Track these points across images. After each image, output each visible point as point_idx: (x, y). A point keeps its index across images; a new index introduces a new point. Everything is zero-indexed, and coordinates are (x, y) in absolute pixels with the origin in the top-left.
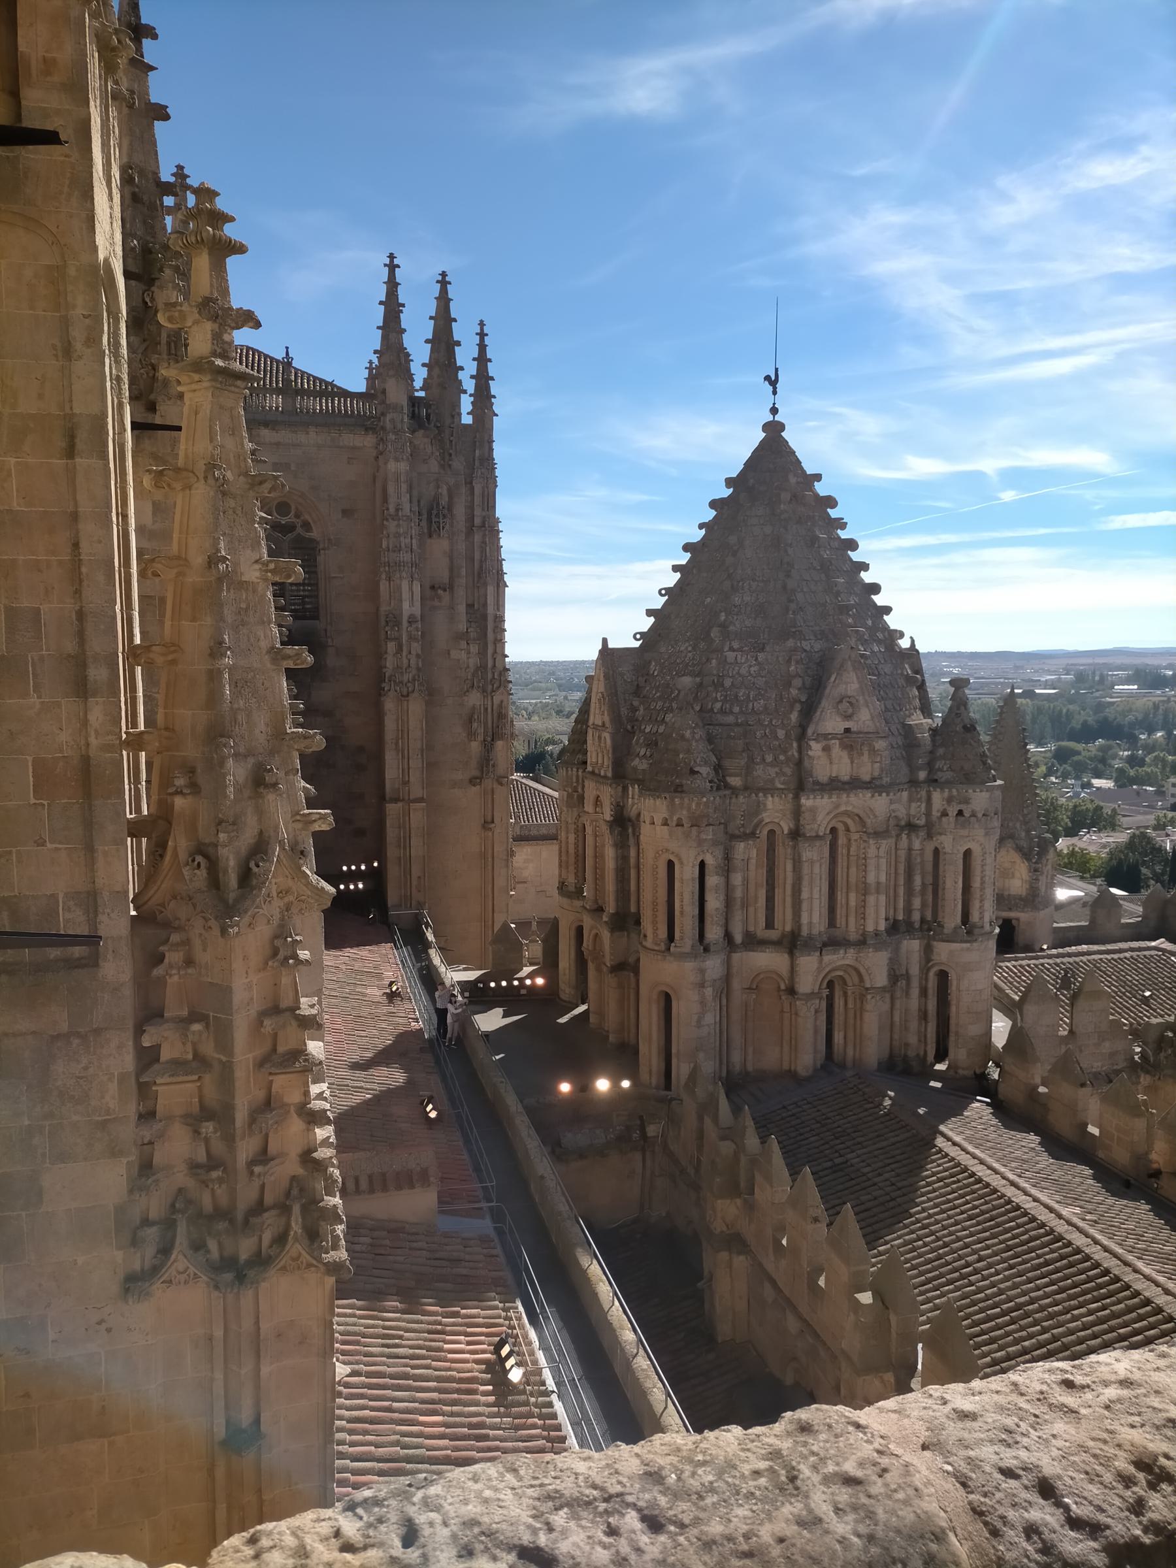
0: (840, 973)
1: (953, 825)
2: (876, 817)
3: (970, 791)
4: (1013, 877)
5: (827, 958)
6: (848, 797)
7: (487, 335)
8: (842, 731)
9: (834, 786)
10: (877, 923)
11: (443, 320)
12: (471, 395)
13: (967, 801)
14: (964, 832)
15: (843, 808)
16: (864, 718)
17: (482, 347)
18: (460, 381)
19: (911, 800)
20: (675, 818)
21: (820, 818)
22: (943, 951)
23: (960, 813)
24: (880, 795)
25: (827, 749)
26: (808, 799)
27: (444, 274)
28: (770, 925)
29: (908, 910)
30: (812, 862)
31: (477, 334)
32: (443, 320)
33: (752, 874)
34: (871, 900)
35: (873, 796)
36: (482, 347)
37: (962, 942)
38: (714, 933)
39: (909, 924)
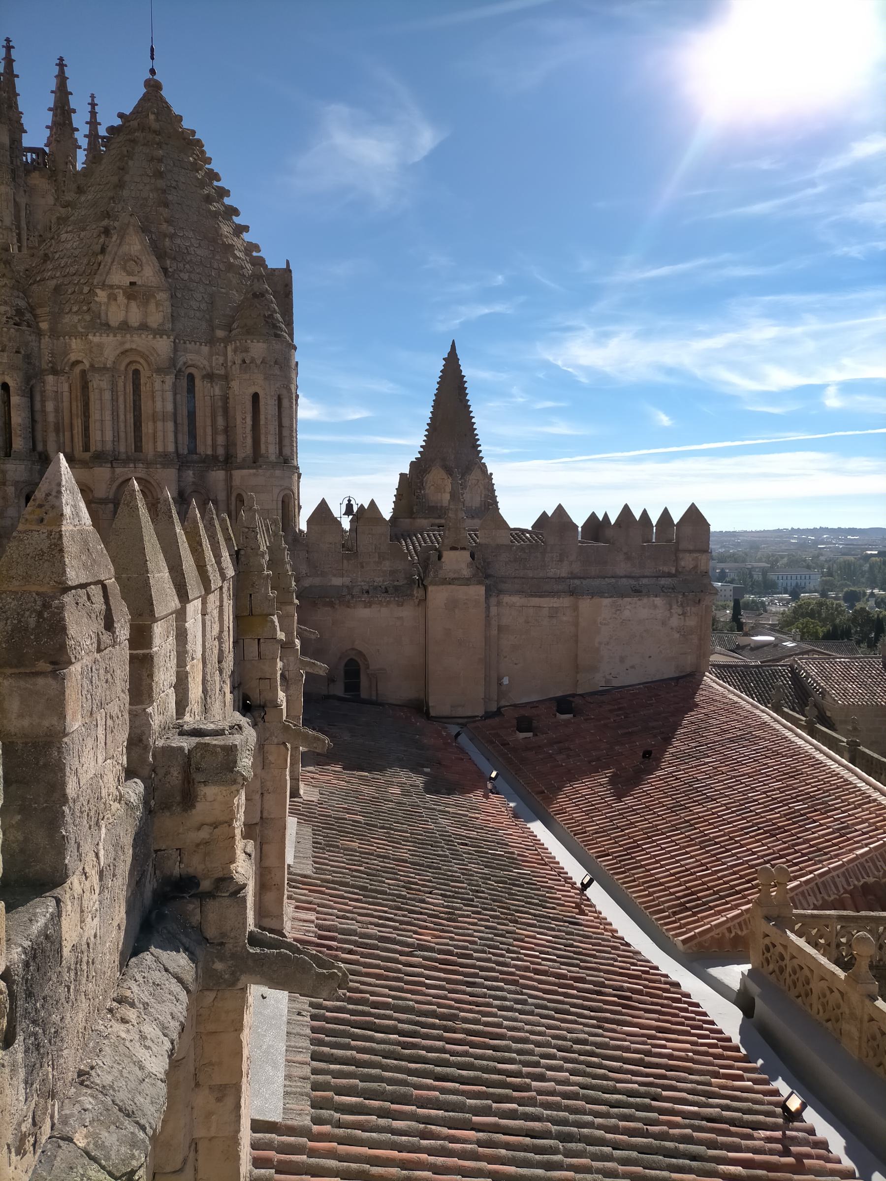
2: (158, 355)
3: (249, 341)
4: (445, 492)
5: (118, 471)
6: (132, 336)
7: (97, 105)
8: (128, 284)
10: (165, 446)
11: (62, 92)
12: (85, 150)
13: (246, 350)
14: (247, 376)
15: (127, 346)
16: (147, 275)
17: (93, 114)
18: (76, 140)
21: (106, 353)
23: (244, 361)
24: (161, 337)
25: (112, 297)
26: (94, 335)
27: (61, 59)
28: (86, 448)
30: (101, 391)
31: (89, 104)
32: (62, 92)
34: (159, 424)
35: (154, 337)
36: (93, 114)
37: (249, 468)
39: (215, 457)
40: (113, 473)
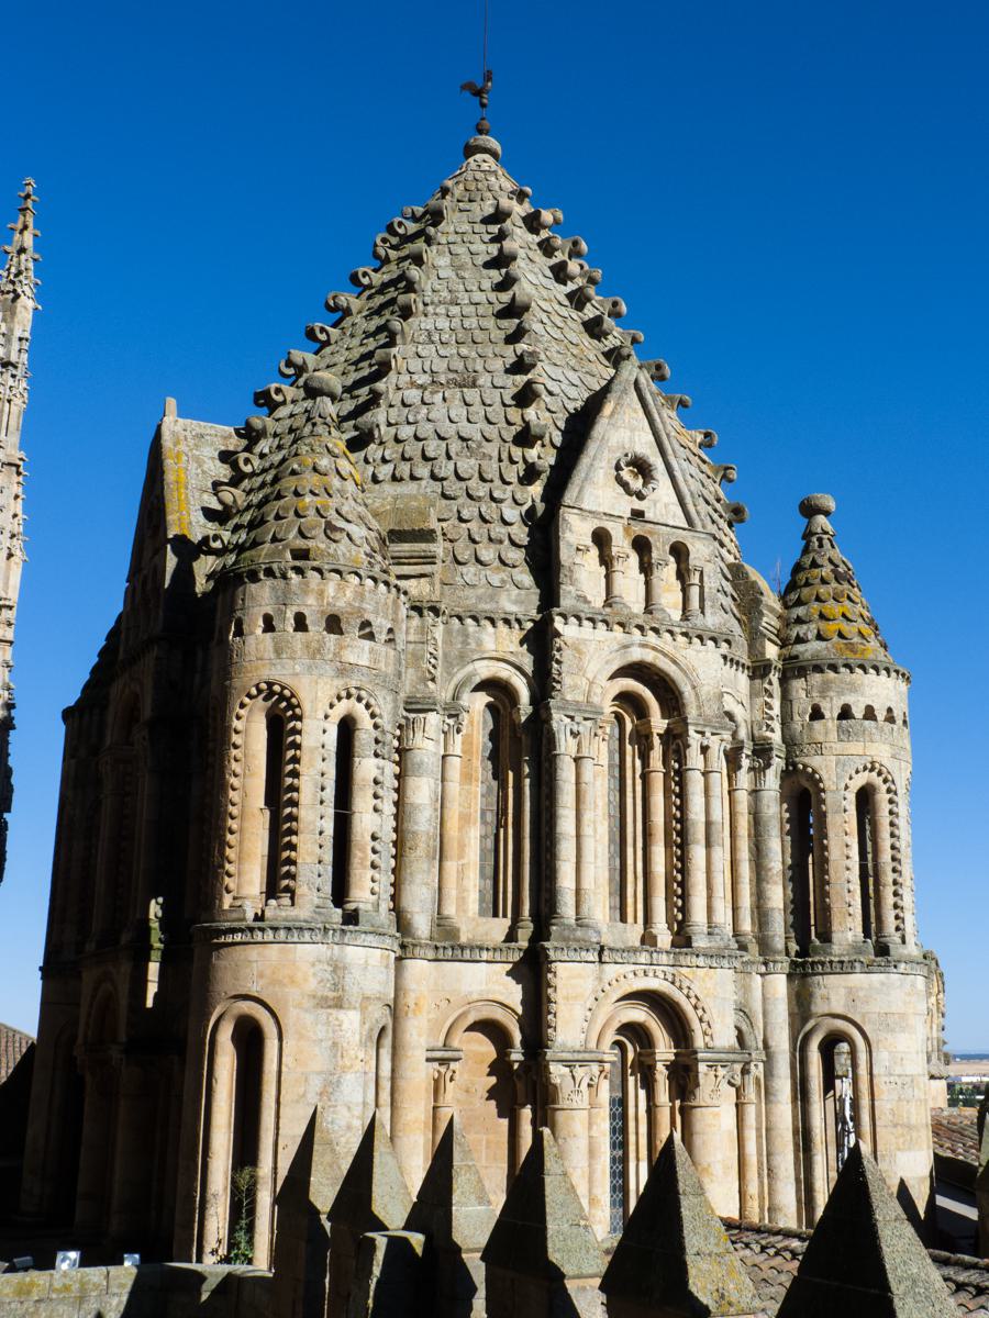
0: (639, 1014)
1: (833, 736)
5: (611, 971)
8: (629, 515)
9: (609, 614)
14: (855, 747)
15: (637, 654)
16: (665, 499)
19: (753, 694)
20: (290, 615)
22: (833, 993)
23: (846, 713)
25: (601, 539)
29: (761, 913)
33: (454, 787)
34: (698, 853)
38: (367, 889)
40: (600, 979)
